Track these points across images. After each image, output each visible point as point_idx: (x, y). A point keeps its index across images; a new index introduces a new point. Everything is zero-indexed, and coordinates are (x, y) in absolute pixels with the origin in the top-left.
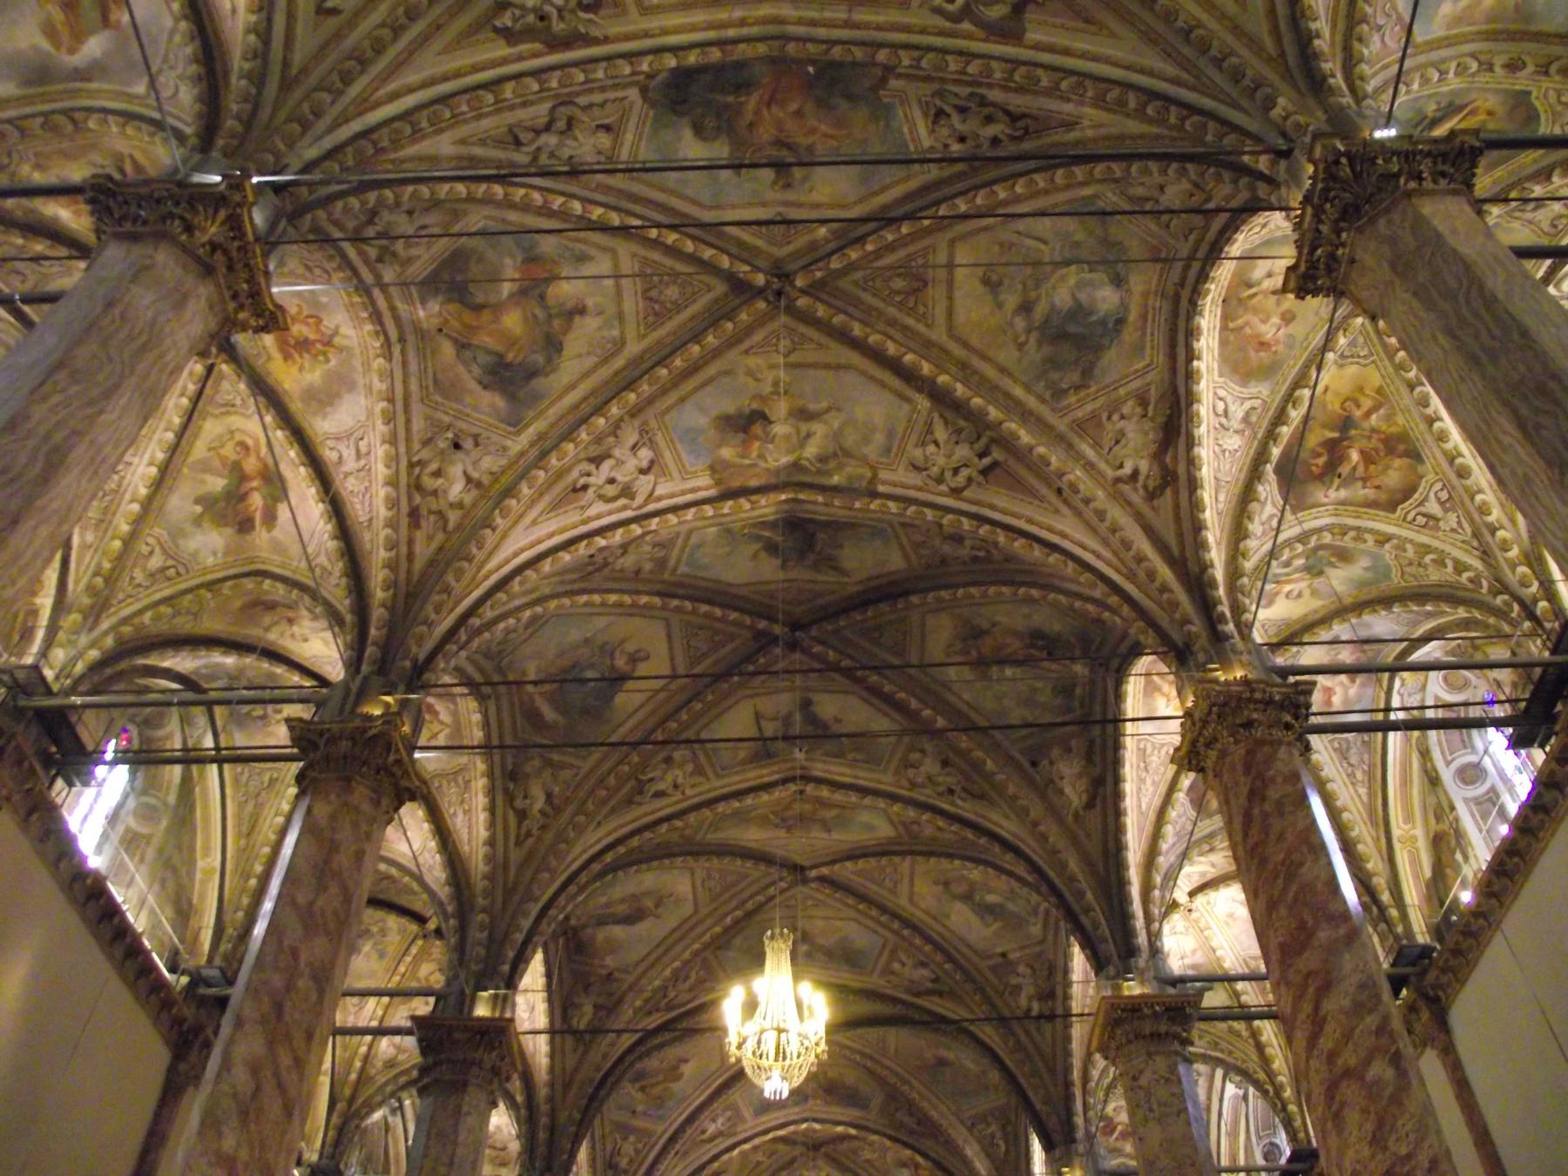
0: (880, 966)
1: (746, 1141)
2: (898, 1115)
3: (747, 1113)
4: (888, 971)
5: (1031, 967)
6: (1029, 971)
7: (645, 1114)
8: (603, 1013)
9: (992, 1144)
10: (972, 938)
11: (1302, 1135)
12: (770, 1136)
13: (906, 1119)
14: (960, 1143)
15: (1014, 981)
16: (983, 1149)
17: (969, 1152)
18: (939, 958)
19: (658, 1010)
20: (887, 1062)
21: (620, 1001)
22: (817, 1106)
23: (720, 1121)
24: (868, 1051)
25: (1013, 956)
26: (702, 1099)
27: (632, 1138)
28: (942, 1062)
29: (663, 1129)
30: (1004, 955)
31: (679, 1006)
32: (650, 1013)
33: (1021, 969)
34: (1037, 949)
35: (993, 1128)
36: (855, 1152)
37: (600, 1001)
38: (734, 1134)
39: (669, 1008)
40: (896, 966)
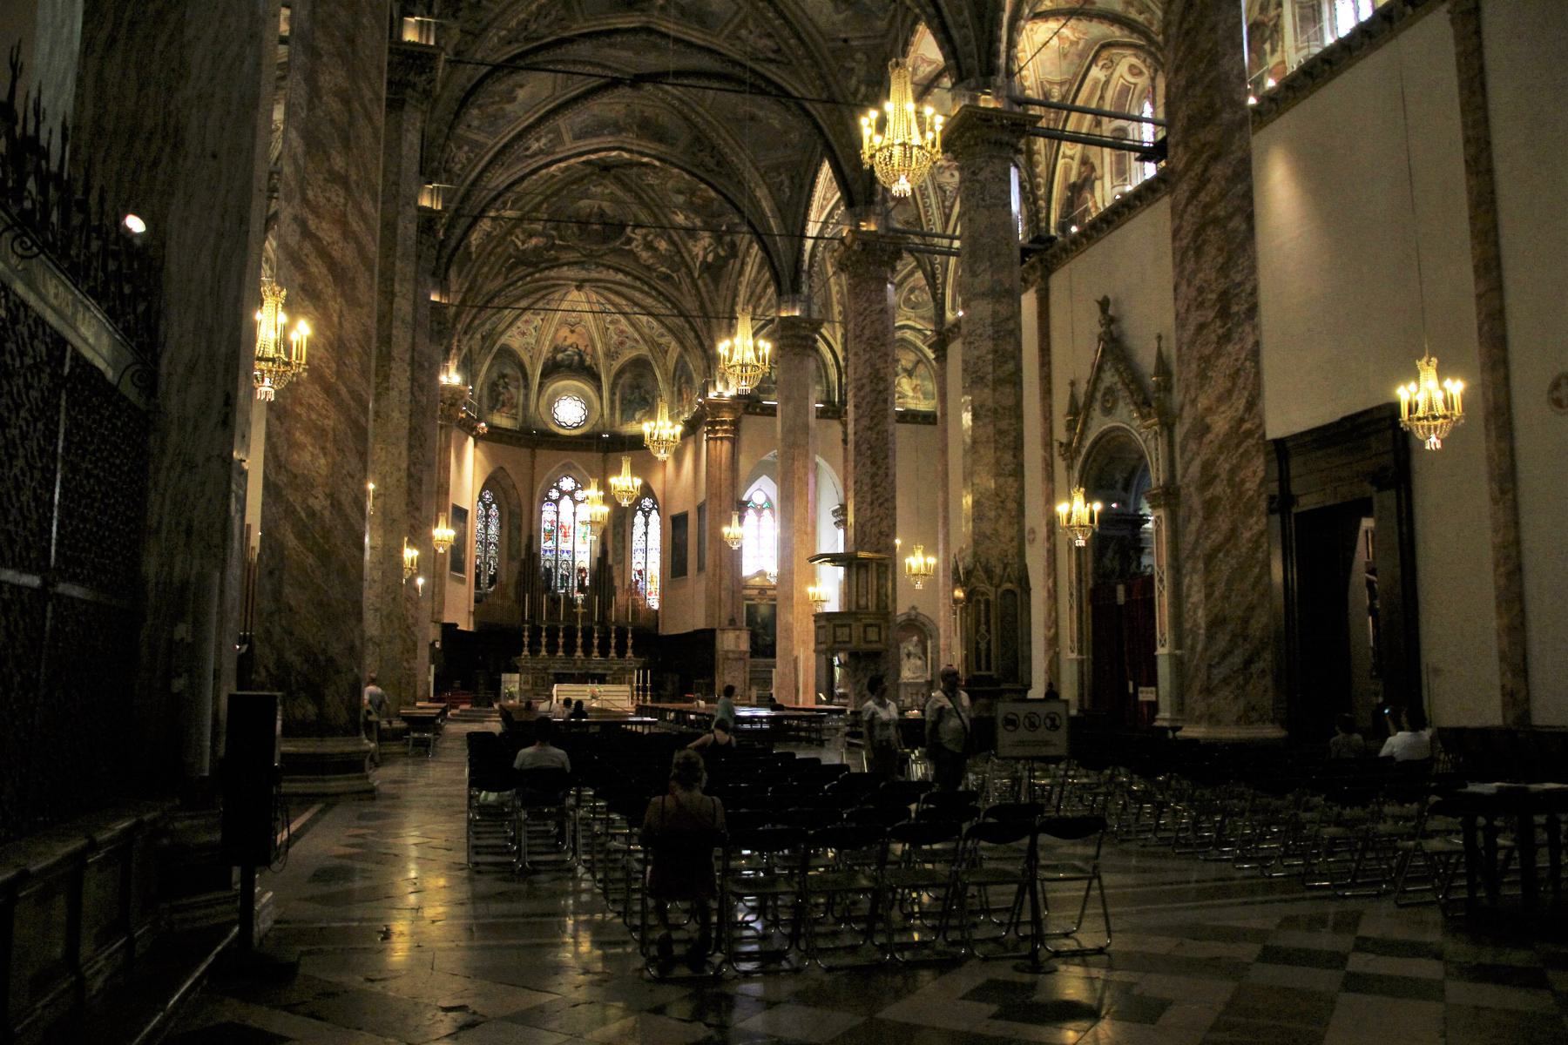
0: (726, 32)
1: (560, 160)
2: (700, 155)
3: (567, 137)
4: (734, 36)
5: (868, 57)
6: (864, 59)
7: (478, 128)
8: (469, 38)
9: (779, 190)
10: (822, 21)
11: (1043, 224)
12: (584, 158)
13: (707, 159)
14: (752, 185)
15: (850, 64)
16: (770, 192)
17: (758, 193)
18: (786, 32)
19: (517, 41)
20: (700, 110)
21: (485, 30)
22: (629, 139)
23: (543, 141)
24: (685, 98)
25: (855, 43)
26: (531, 120)
27: (466, 148)
28: (753, 118)
29: (494, 143)
30: (845, 41)
31: (537, 39)
32: (510, 43)
33: (859, 56)
34: (878, 41)
35: (783, 177)
36: (639, 176)
37: (467, 26)
38: (553, 153)
39: (527, 40)
40: (743, 32)
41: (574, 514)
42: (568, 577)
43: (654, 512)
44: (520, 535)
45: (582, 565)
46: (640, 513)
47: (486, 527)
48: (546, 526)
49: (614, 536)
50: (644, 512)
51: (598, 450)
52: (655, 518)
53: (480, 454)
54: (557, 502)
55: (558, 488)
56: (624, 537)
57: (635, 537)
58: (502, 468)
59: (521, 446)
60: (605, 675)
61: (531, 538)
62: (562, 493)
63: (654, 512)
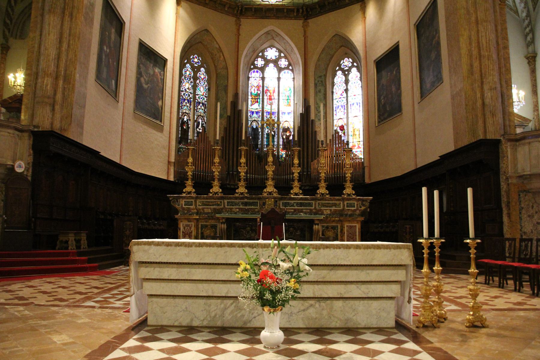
41: (279, 79)
42: (273, 136)
43: (354, 70)
44: (226, 93)
45: (286, 125)
46: (339, 73)
47: (195, 87)
48: (253, 90)
49: (316, 93)
50: (343, 71)
51: (296, 18)
52: (354, 74)
53: (181, 11)
54: (262, 69)
55: (263, 57)
56: (325, 94)
57: (335, 96)
58: (207, 30)
59: (228, 13)
60: (311, 222)
61: (236, 95)
62: (267, 62)
63: (354, 70)
